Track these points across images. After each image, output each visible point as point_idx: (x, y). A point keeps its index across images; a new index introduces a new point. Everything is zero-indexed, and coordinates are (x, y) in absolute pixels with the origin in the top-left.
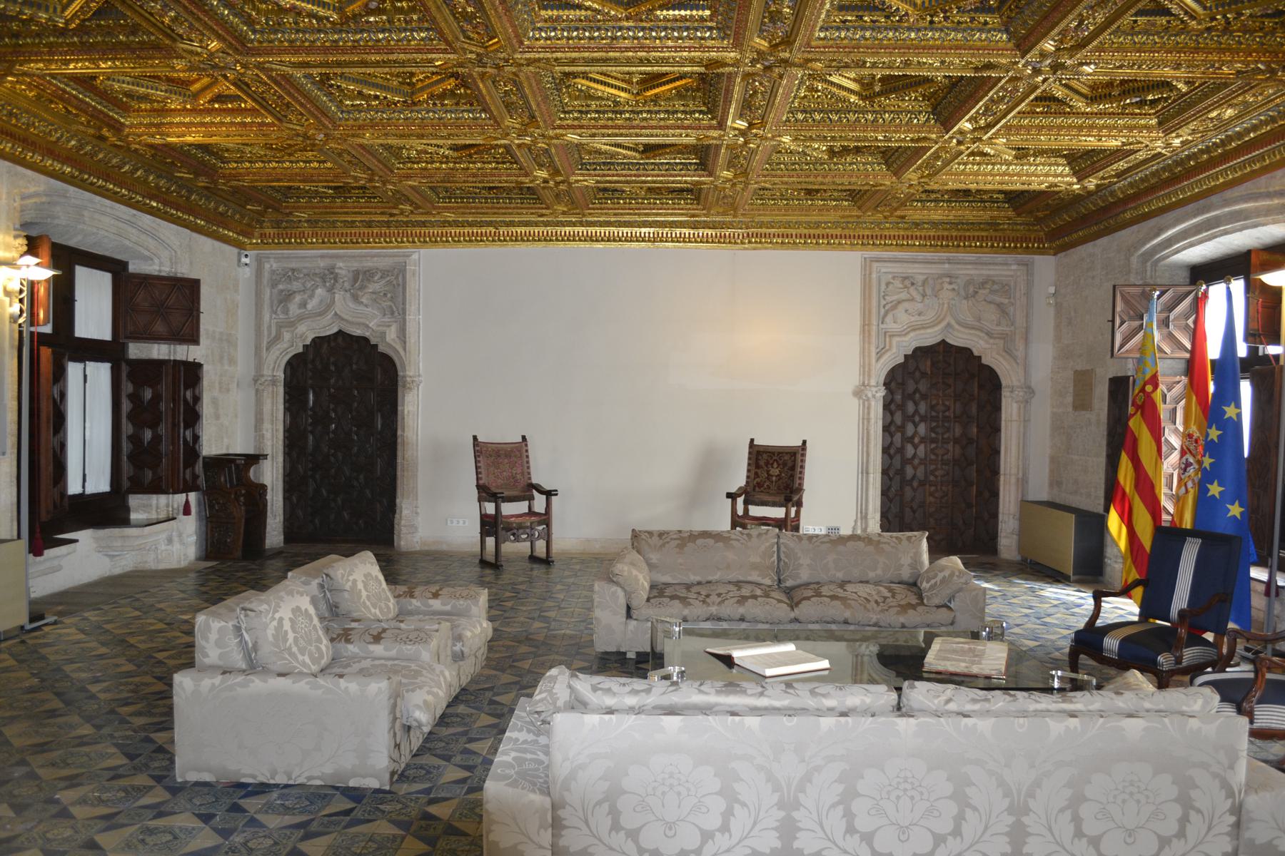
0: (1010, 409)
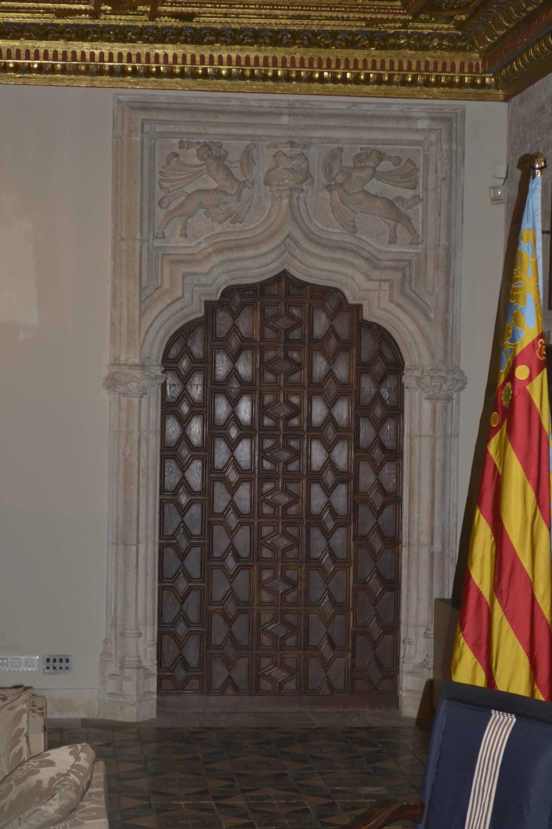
0: (419, 412)
